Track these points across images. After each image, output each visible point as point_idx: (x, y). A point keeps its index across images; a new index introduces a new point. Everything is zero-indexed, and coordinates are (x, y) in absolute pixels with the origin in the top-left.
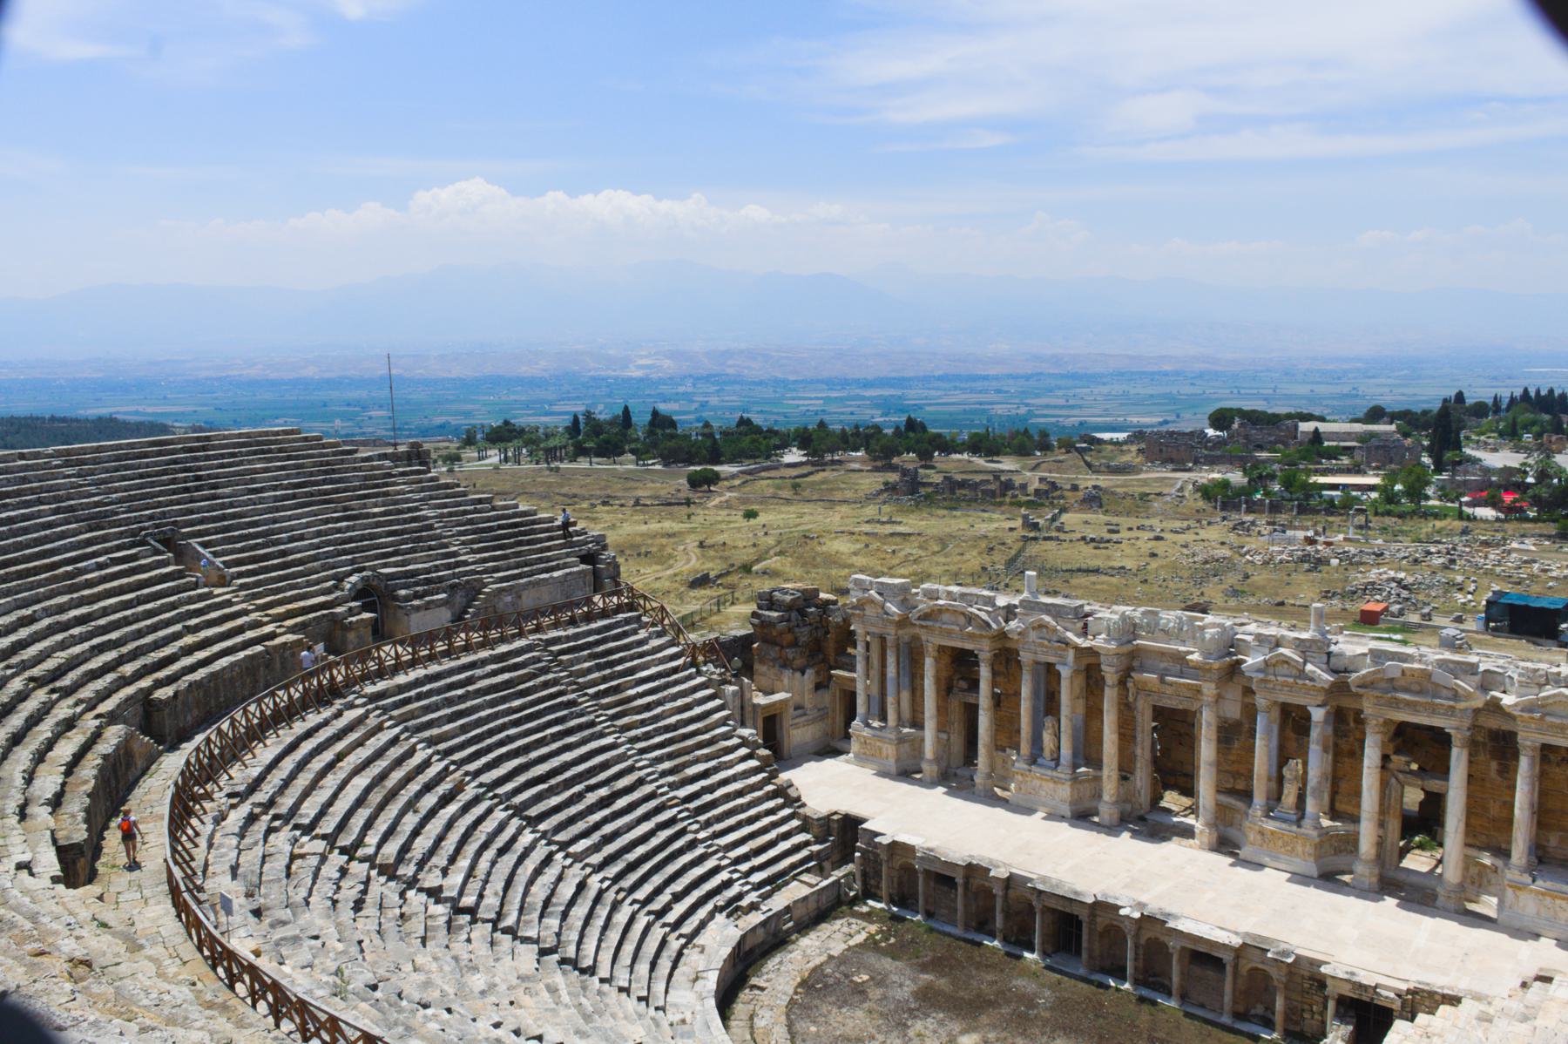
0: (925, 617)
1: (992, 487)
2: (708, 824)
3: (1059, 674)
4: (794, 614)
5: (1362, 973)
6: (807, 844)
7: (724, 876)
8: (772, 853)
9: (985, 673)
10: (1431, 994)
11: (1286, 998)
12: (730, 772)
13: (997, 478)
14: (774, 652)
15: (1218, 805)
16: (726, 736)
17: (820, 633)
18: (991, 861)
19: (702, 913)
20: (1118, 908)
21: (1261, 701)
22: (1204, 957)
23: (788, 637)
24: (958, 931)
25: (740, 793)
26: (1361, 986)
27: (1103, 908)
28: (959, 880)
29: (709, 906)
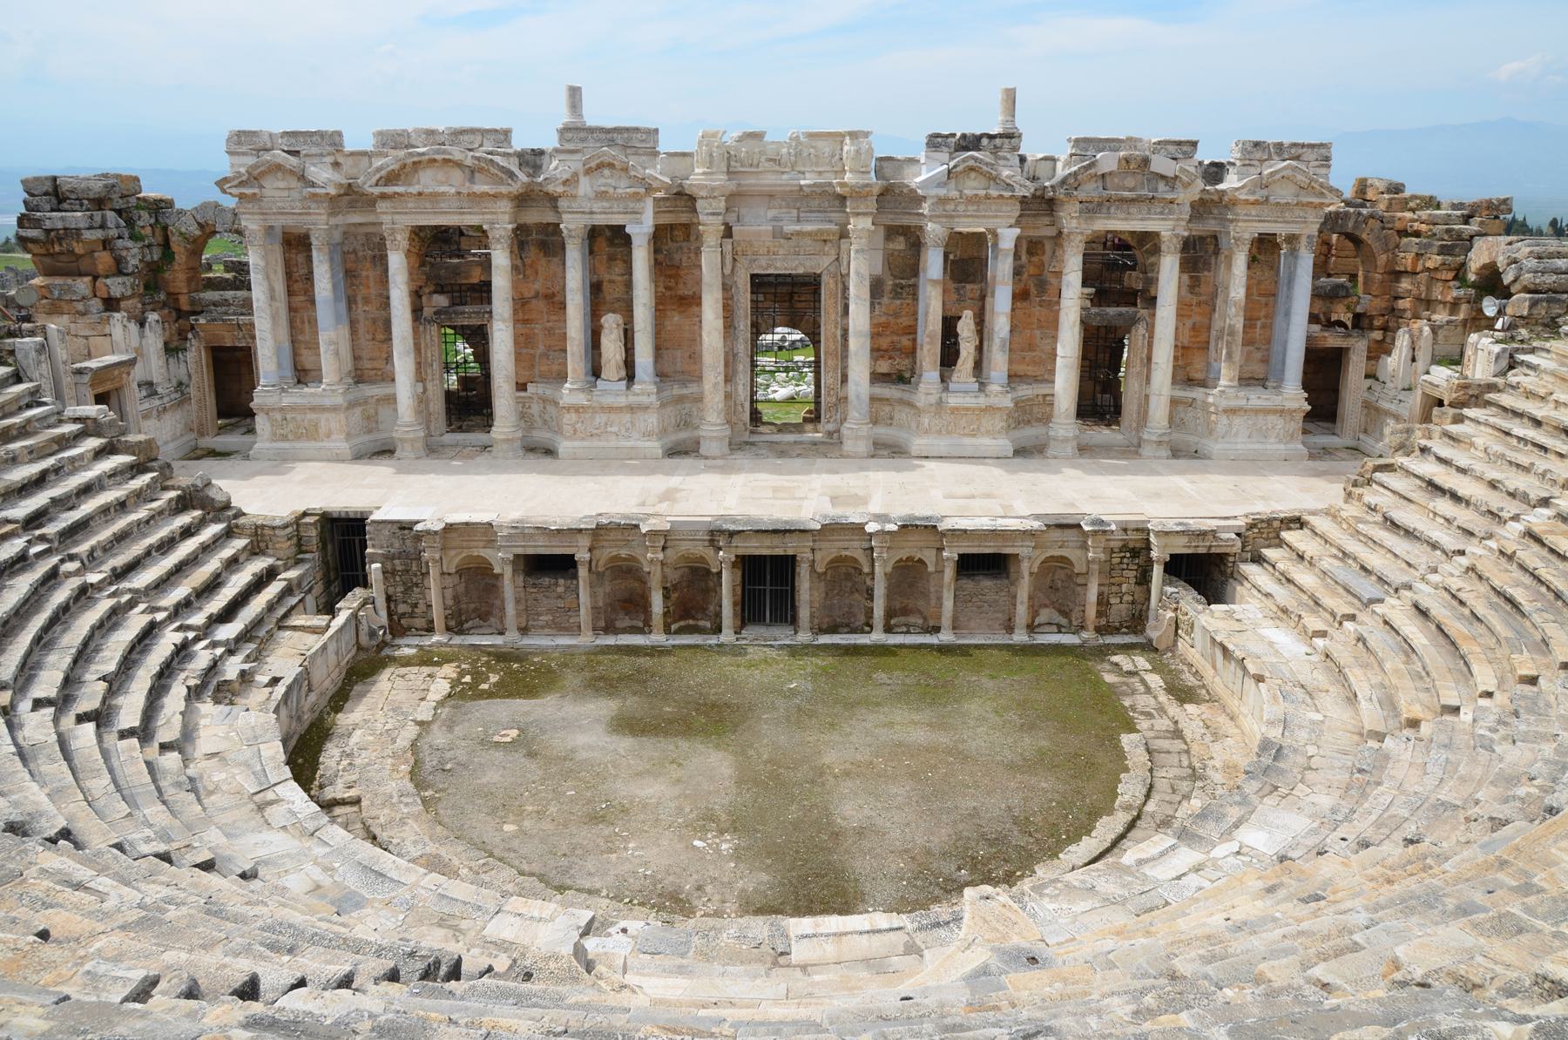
0: (391, 178)
3: (627, 240)
6: (270, 575)
9: (501, 259)
10: (1269, 521)
14: (82, 285)
17: (156, 255)
20: (859, 528)
21: (934, 230)
22: (985, 563)
24: (586, 639)
26: (1202, 534)
28: (582, 555)
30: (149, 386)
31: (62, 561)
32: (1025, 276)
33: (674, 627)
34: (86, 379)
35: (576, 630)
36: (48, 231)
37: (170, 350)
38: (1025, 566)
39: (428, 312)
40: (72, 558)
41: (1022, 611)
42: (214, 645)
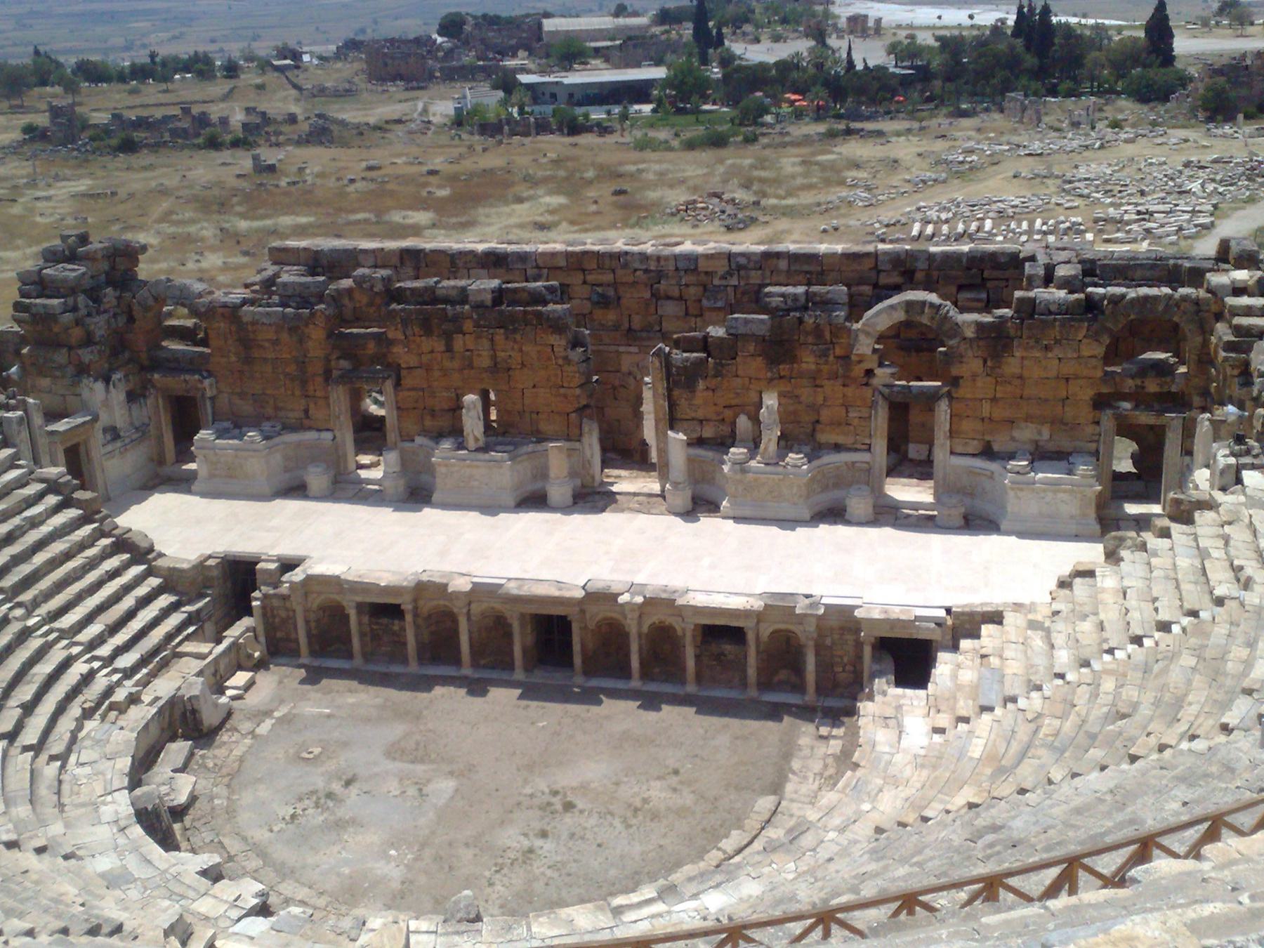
1: (185, 124)
2: (36, 603)
4: (81, 299)
5: (897, 609)
7: (80, 668)
8: (136, 625)
11: (817, 654)
12: (45, 529)
13: (186, 111)
14: (61, 357)
15: (690, 460)
16: (21, 483)
17: (122, 320)
18: (444, 574)
19: (66, 724)
20: (615, 596)
23: (77, 333)
25: (67, 556)
27: (600, 597)
28: (407, 607)
29: (75, 710)
30: (113, 433)
31: (11, 609)
32: (831, 358)
33: (482, 662)
34: (56, 438)
35: (405, 661)
36: (34, 316)
37: (132, 397)
38: (751, 637)
39: (335, 373)
40: (19, 605)
41: (752, 672)
42: (115, 671)
